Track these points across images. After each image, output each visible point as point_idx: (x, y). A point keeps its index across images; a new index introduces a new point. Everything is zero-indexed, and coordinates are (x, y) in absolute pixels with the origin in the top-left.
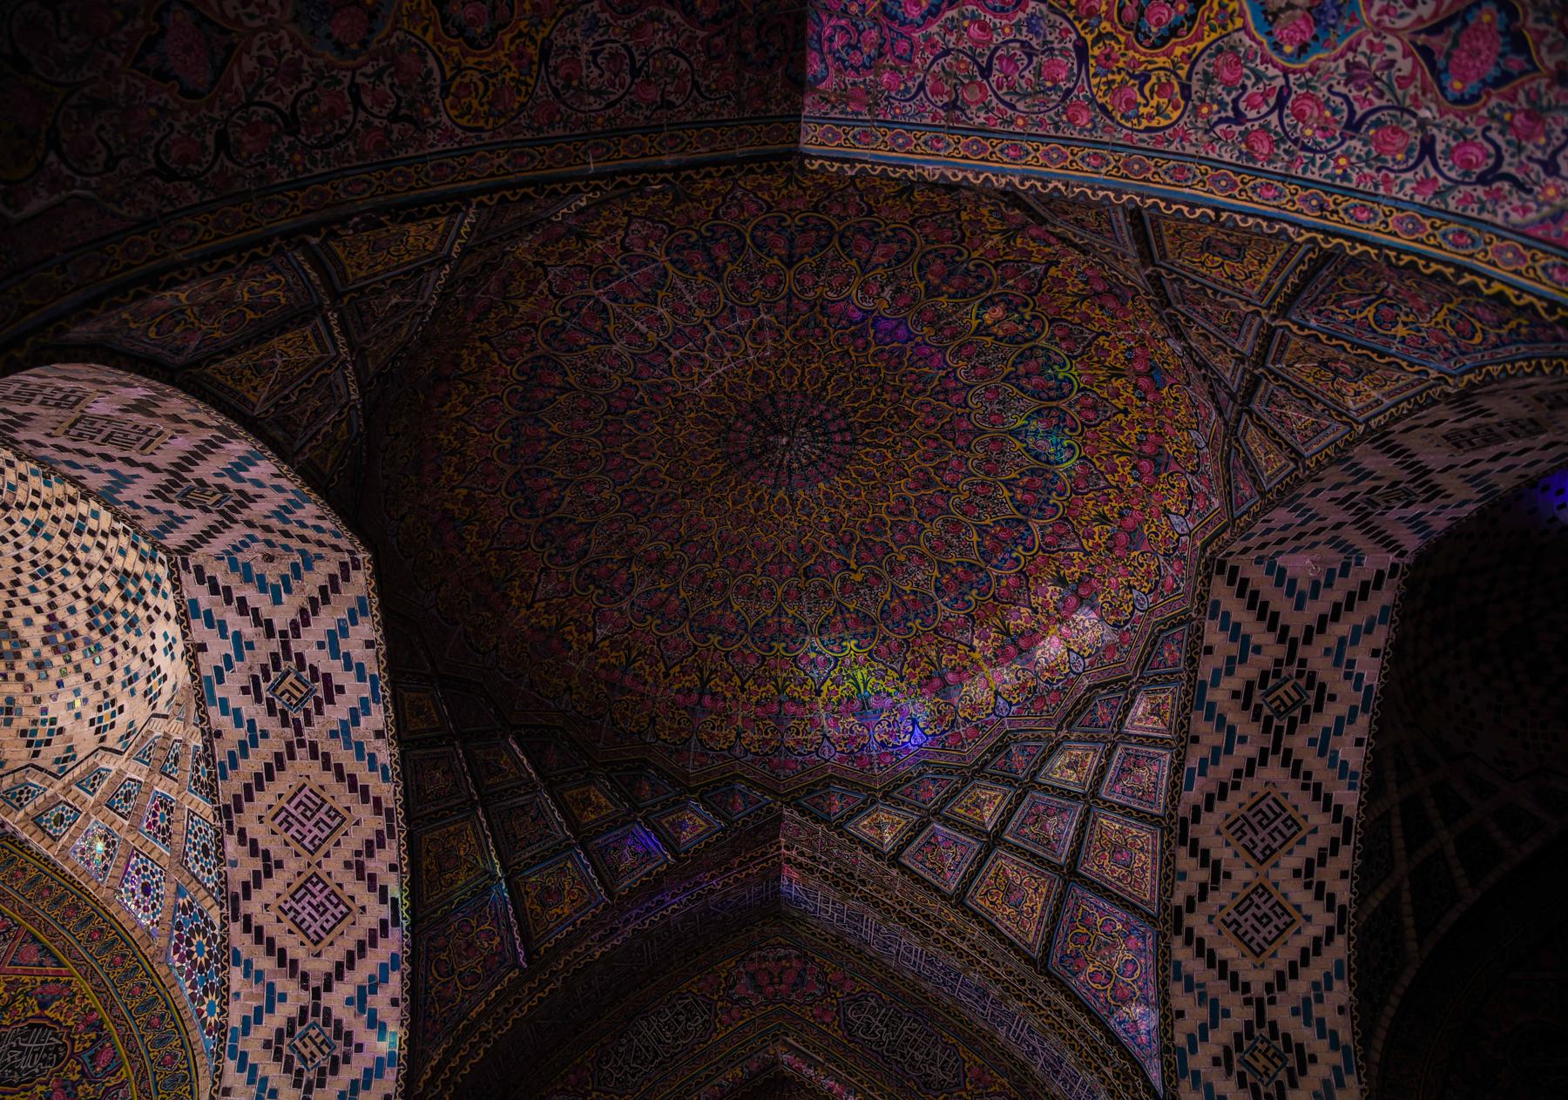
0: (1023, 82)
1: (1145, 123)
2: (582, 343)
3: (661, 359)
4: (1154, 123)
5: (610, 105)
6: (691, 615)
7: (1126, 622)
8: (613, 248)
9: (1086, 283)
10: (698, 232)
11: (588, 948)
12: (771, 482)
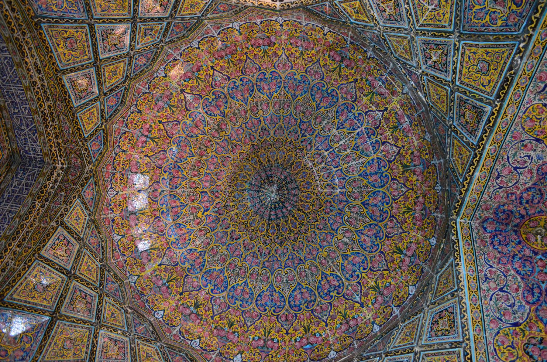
0: (501, 303)
1: (497, 348)
2: (340, 117)
3: (324, 147)
4: (498, 352)
5: (508, 158)
6: (188, 138)
7: (183, 337)
8: (386, 138)
9: (353, 318)
10: (387, 171)
11: (33, 56)
12: (253, 182)
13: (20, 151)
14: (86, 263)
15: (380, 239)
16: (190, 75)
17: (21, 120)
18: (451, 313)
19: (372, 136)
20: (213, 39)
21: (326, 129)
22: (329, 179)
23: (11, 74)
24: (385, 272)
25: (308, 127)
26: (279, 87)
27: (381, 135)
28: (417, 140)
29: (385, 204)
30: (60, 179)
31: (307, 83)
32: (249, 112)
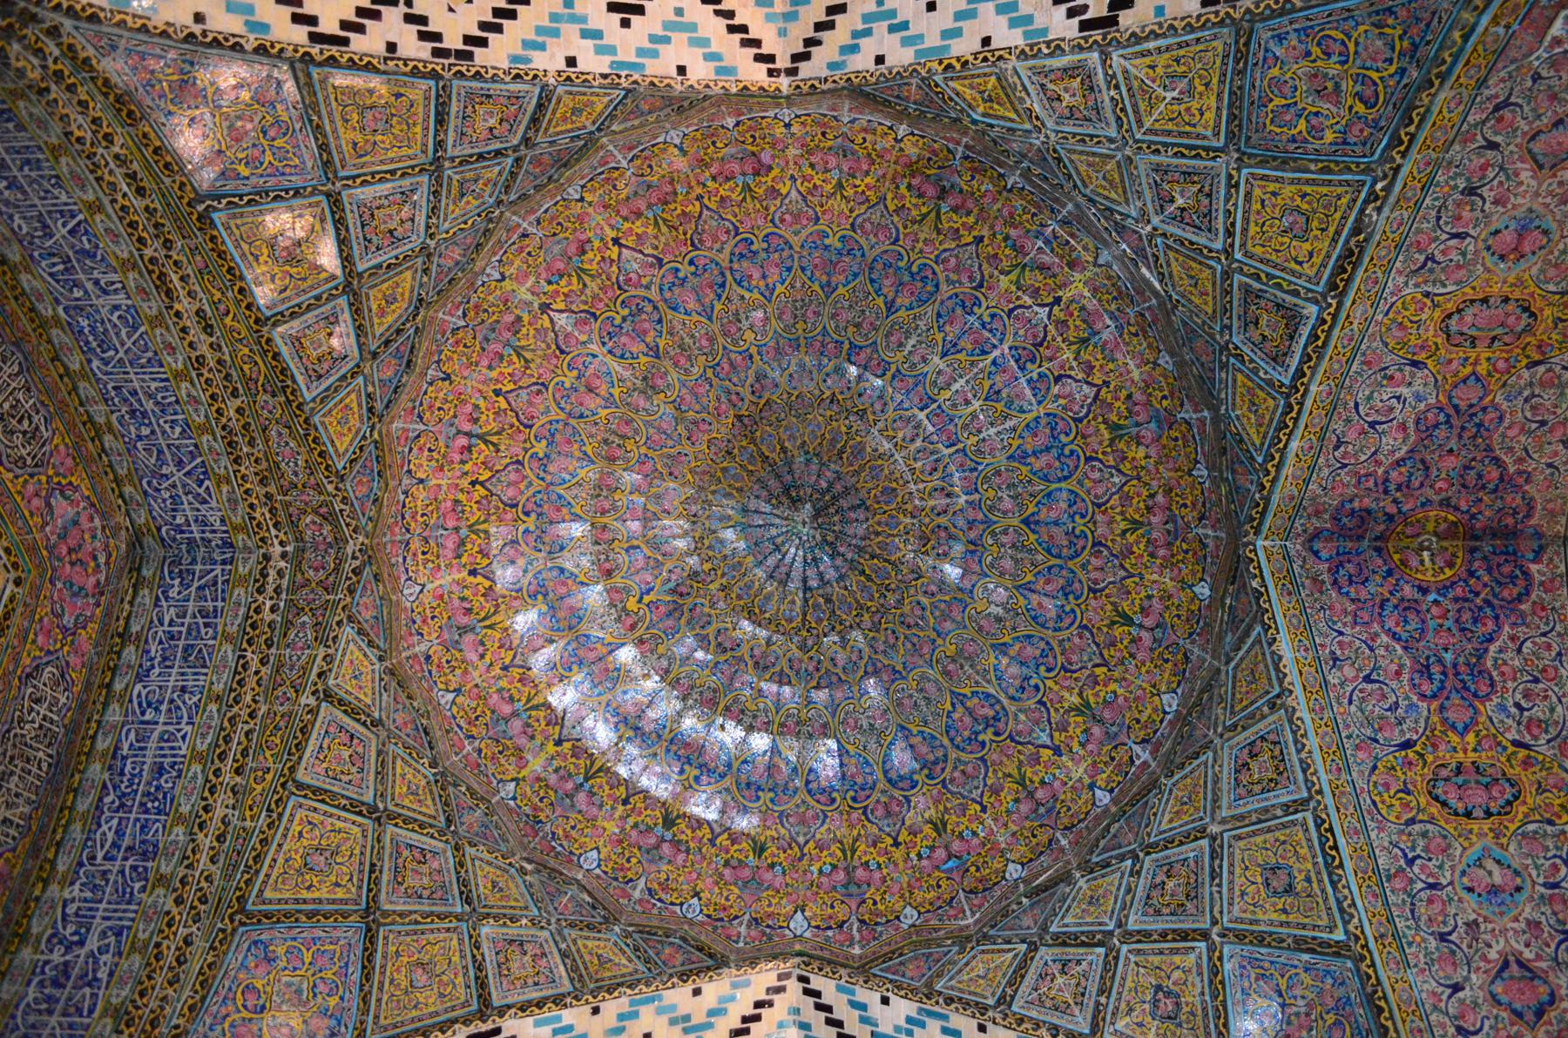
1: (1377, 799)
2: (948, 328)
3: (916, 400)
5: (1357, 405)
6: (572, 422)
7: (660, 900)
8: (1062, 367)
9: (1043, 782)
13: (159, 529)
14: (403, 776)
15: (1077, 598)
16: (561, 265)
17: (160, 452)
18: (1275, 743)
19: (1029, 365)
20: (616, 174)
21: (916, 359)
22: (936, 475)
23: (129, 344)
24: (1098, 671)
25: (871, 359)
26: (789, 270)
27: (1051, 359)
28: (1138, 366)
29: (1077, 518)
30: (285, 582)
31: (858, 254)
32: (721, 340)
